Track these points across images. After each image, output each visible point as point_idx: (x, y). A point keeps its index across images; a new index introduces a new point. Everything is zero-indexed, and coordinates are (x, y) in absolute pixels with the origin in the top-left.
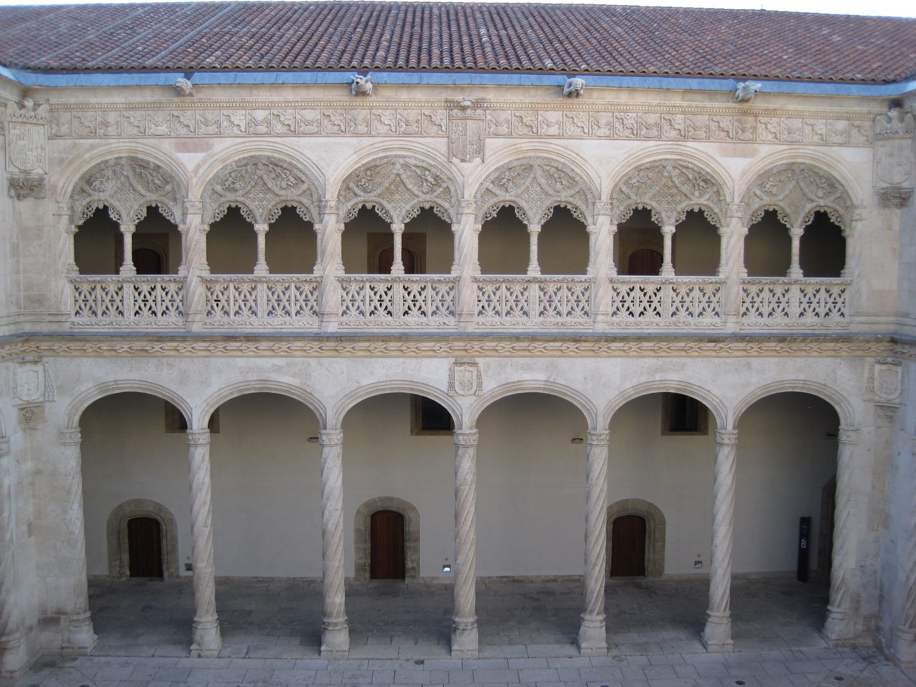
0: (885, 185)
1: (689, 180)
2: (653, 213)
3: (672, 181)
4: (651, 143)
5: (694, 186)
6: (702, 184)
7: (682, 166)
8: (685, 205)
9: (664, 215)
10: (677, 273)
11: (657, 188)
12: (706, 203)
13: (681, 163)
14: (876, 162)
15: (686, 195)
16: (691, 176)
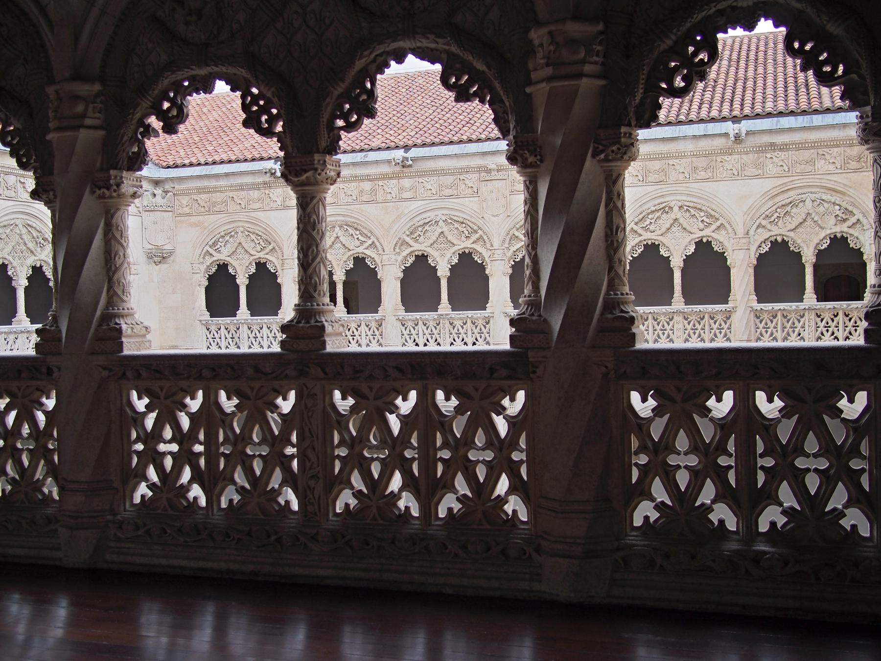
0: (151, 247)
1: (33, 238)
2: (9, 267)
3: (22, 239)
4: (11, 203)
5: (37, 243)
6: (42, 242)
7: (29, 225)
8: (31, 261)
9: (18, 269)
10: (686, 303)
11: (13, 244)
12: (45, 259)
13: (29, 222)
14: (143, 228)
15: (32, 252)
16: (35, 235)
